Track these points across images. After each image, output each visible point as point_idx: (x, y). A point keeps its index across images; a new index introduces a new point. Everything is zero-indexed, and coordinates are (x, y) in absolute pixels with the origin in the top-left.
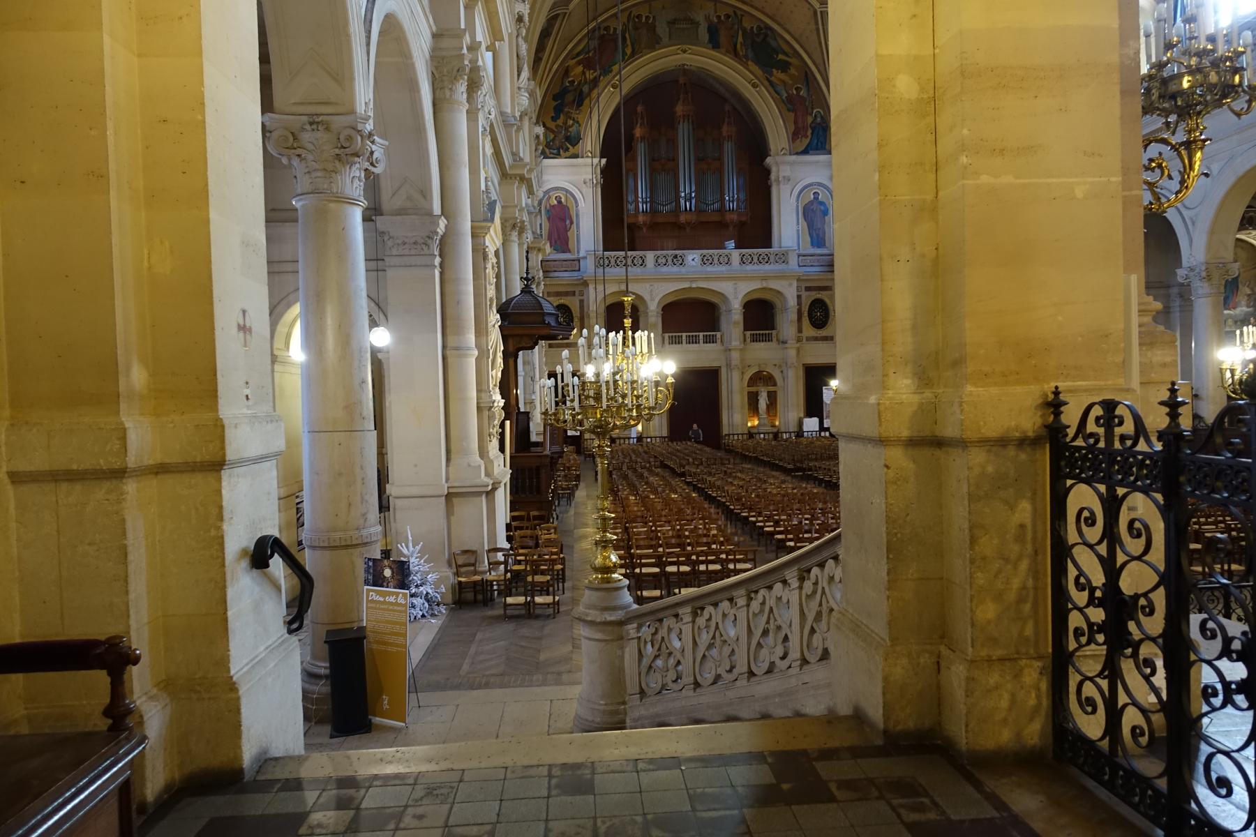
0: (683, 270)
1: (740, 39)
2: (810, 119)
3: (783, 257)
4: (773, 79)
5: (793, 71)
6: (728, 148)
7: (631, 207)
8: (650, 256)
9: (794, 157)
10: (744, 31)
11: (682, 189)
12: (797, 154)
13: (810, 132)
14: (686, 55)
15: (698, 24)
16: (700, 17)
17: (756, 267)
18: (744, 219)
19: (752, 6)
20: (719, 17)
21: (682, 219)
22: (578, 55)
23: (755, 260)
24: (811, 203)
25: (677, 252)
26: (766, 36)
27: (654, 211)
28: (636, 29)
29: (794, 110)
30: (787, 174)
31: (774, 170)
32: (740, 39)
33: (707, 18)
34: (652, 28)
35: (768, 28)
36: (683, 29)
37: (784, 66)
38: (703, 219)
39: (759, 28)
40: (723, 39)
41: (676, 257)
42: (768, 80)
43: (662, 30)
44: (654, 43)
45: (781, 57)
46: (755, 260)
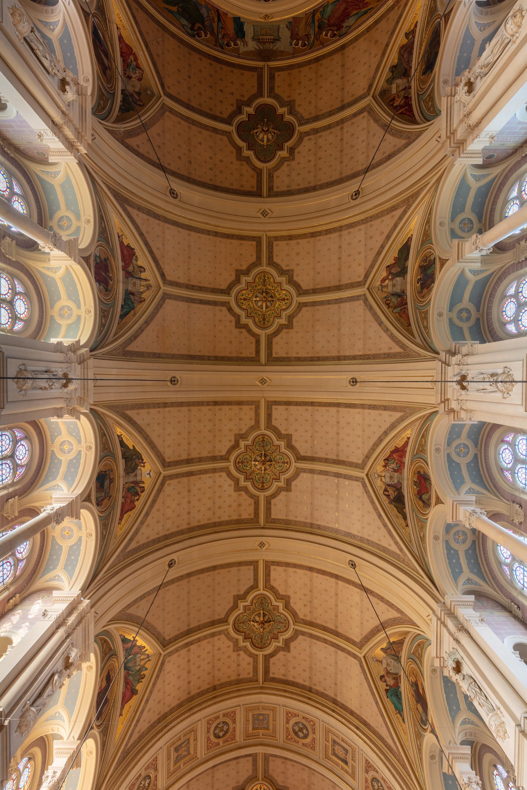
1: (215, 25)
15: (253, 39)
16: (252, 45)
20: (235, 44)
22: (366, 12)
28: (308, 36)
33: (246, 44)
34: (294, 36)
35: (192, 36)
43: (285, 34)
45: (175, 9)
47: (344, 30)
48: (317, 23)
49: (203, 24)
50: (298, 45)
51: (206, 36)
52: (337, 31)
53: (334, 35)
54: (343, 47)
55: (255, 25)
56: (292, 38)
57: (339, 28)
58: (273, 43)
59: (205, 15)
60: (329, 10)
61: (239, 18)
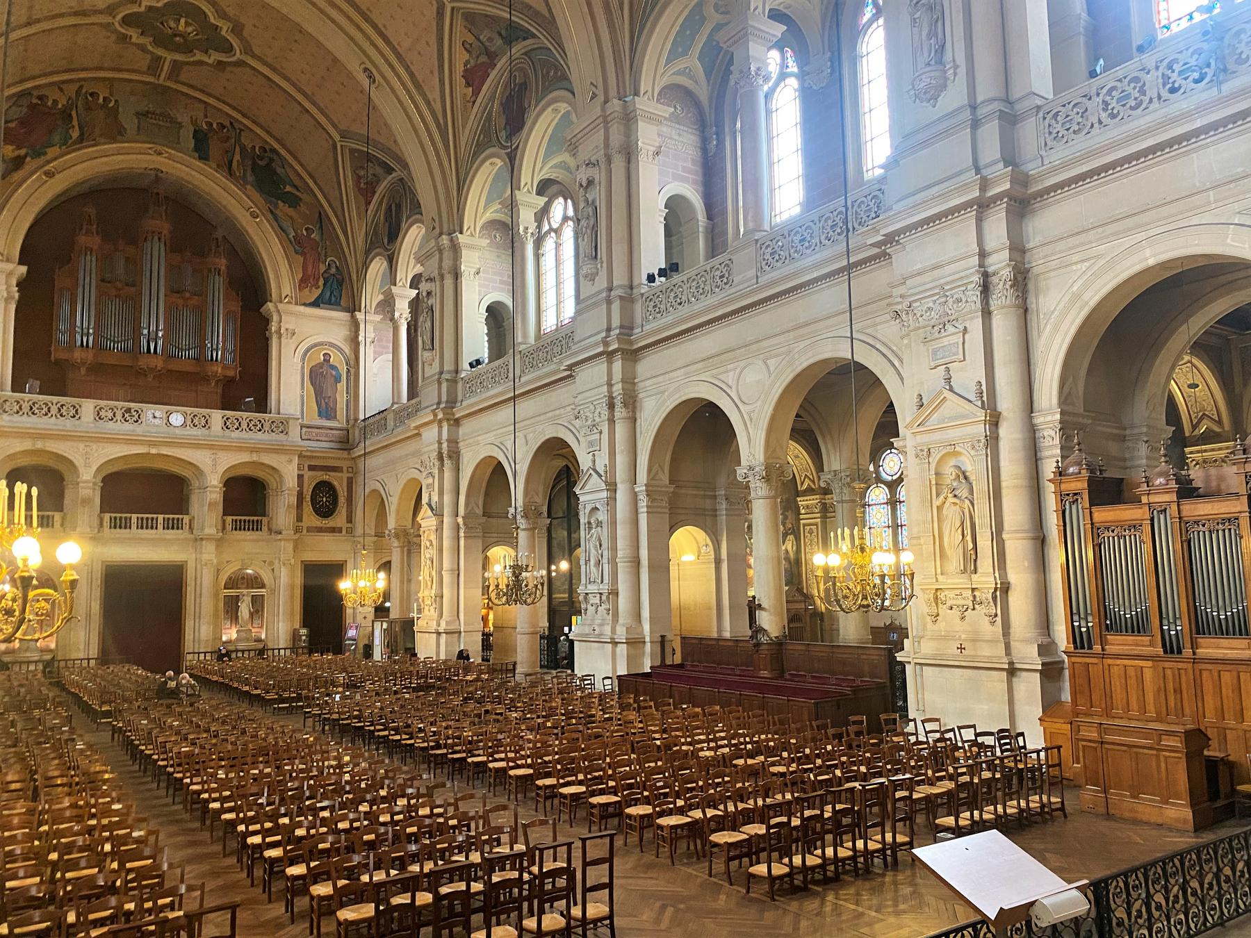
0: (139, 429)
1: (237, 157)
2: (323, 268)
3: (282, 425)
4: (278, 212)
5: (303, 208)
6: (218, 284)
7: (63, 338)
8: (88, 407)
9: (302, 308)
10: (243, 149)
11: (144, 324)
12: (305, 304)
13: (321, 282)
14: (159, 158)
15: (180, 125)
16: (184, 118)
17: (245, 435)
18: (231, 373)
19: (254, 122)
21: (143, 362)
23: (244, 426)
24: (320, 365)
25: (132, 405)
26: (272, 160)
27: (99, 348)
28: (88, 109)
29: (303, 254)
30: (291, 327)
31: (275, 318)
32: (237, 157)
33: (194, 122)
35: (274, 151)
36: (157, 122)
37: (293, 201)
38: (173, 366)
39: (263, 149)
40: (215, 149)
41: (128, 411)
42: (271, 212)
43: (128, 121)
44: (116, 133)
45: (288, 188)
46: (244, 426)
47: (25, 102)
48: (75, 122)
49: (254, 164)
50: (105, 99)
51: (254, 147)
52: (37, 104)
53: (40, 98)
54: (22, 81)
55: (175, 144)
56: (115, 111)
57: (33, 107)
58: (148, 112)
59: (249, 172)
60: (56, 138)
61: (200, 158)
